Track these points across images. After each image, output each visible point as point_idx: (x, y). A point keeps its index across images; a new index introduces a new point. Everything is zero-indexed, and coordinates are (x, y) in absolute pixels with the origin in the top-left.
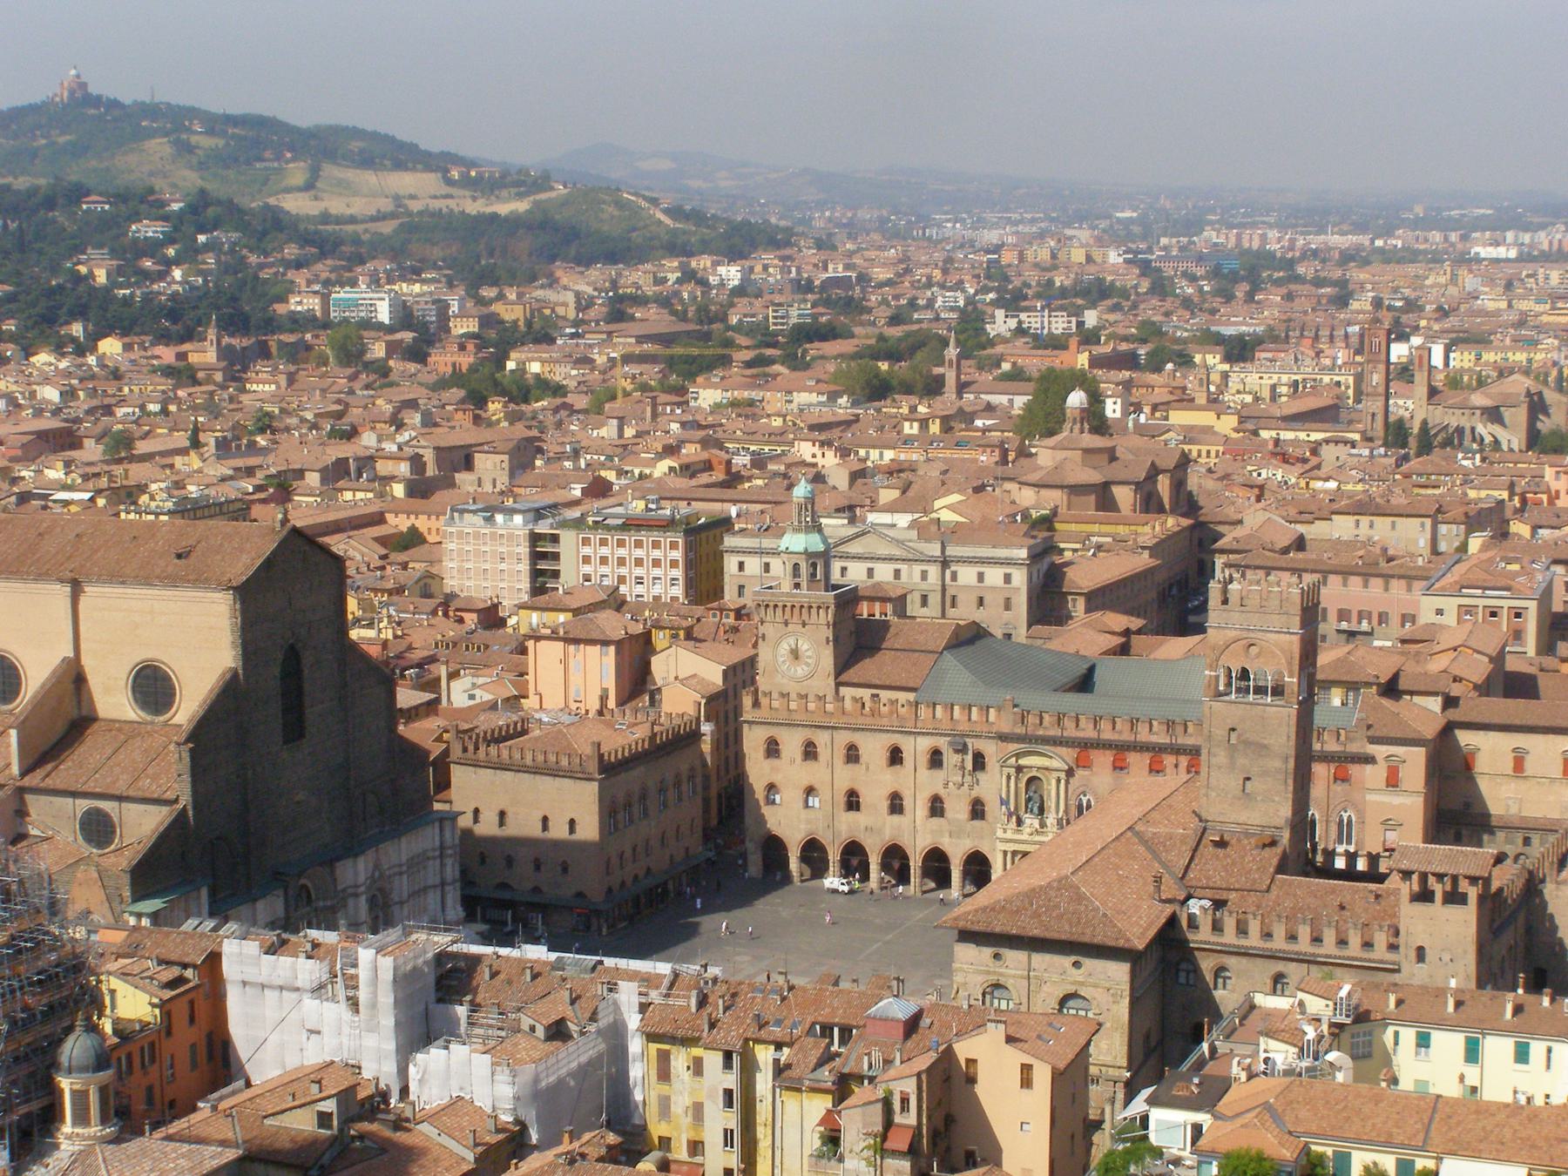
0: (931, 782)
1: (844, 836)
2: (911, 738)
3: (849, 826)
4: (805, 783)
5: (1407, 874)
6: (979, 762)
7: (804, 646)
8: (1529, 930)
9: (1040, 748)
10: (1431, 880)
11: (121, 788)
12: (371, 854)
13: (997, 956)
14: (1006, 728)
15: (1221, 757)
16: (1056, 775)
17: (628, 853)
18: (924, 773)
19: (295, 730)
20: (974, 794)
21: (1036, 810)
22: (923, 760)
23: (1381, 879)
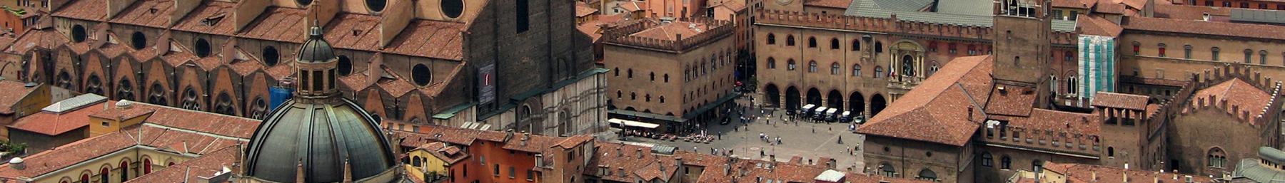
1: (808, 85)
3: (811, 79)
5: (1102, 108)
6: (879, 48)
8: (1168, 140)
10: (1115, 112)
11: (433, 54)
12: (561, 91)
13: (887, 149)
14: (891, 28)
15: (1003, 46)
17: (695, 93)
18: (850, 53)
19: (523, 25)
22: (849, 46)
23: (1090, 111)
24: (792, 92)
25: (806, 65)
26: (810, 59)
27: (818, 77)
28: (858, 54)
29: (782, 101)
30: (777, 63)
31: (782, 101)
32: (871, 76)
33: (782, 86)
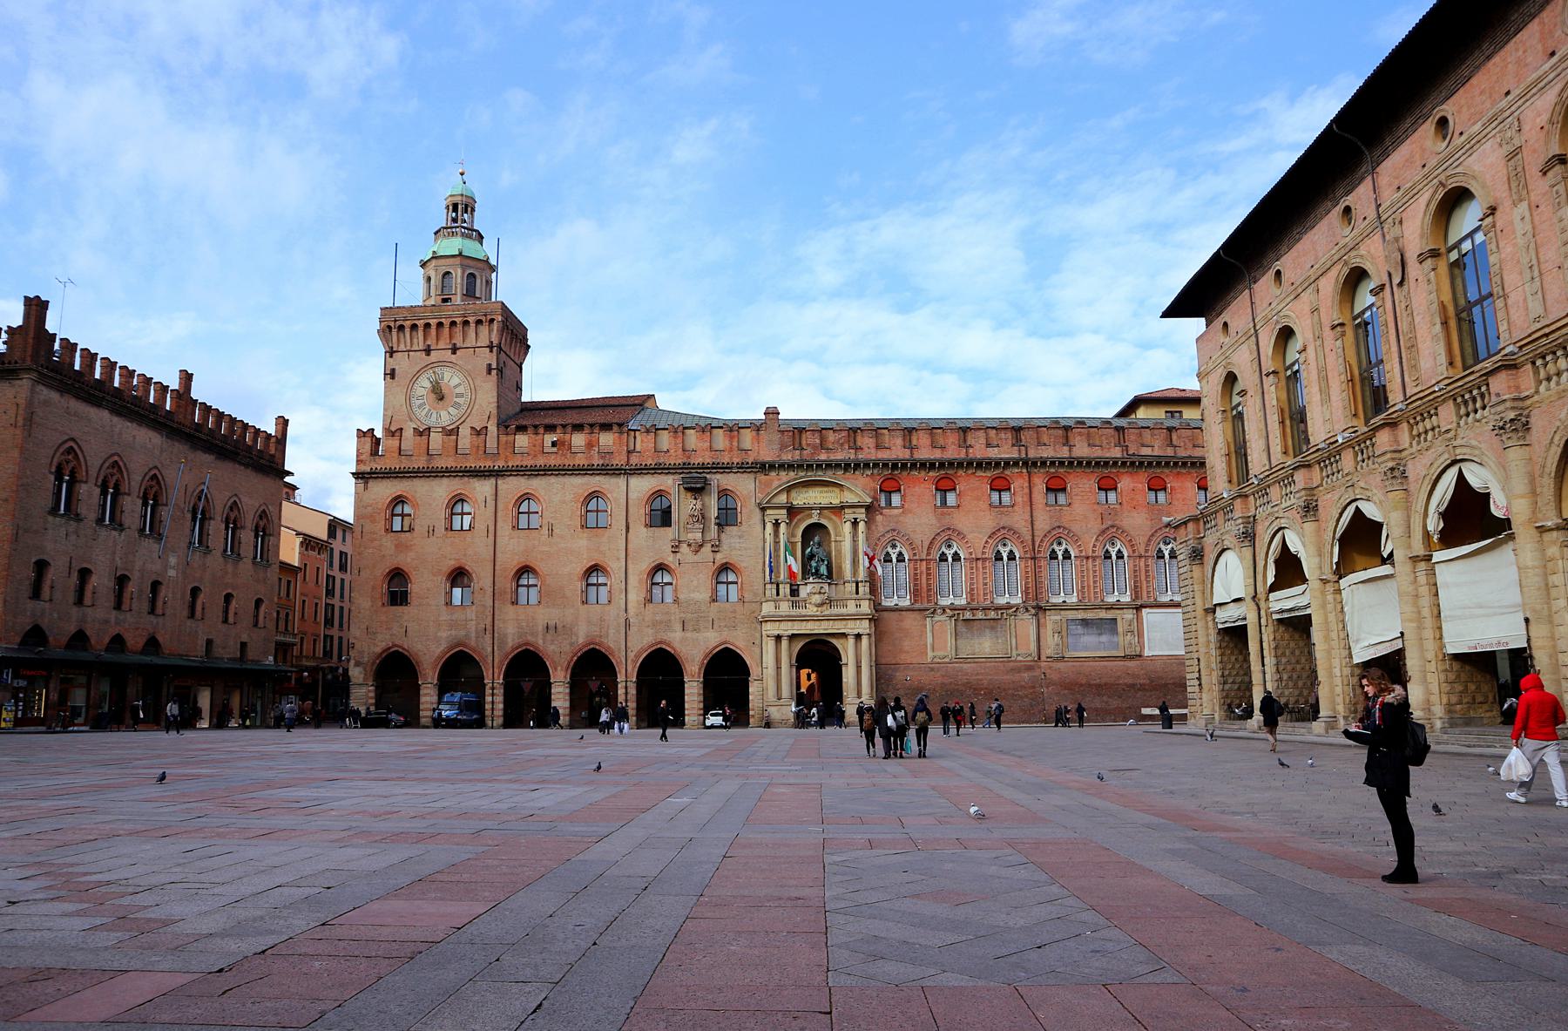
0: (651, 544)
2: (621, 481)
3: (521, 623)
4: (451, 564)
7: (451, 379)
9: (827, 476)
14: (767, 454)
16: (849, 515)
17: (101, 581)
18: (640, 533)
20: (720, 558)
21: (823, 570)
22: (639, 514)
24: (460, 669)
25: (506, 583)
27: (544, 615)
30: (415, 588)
32: (704, 595)
33: (429, 651)
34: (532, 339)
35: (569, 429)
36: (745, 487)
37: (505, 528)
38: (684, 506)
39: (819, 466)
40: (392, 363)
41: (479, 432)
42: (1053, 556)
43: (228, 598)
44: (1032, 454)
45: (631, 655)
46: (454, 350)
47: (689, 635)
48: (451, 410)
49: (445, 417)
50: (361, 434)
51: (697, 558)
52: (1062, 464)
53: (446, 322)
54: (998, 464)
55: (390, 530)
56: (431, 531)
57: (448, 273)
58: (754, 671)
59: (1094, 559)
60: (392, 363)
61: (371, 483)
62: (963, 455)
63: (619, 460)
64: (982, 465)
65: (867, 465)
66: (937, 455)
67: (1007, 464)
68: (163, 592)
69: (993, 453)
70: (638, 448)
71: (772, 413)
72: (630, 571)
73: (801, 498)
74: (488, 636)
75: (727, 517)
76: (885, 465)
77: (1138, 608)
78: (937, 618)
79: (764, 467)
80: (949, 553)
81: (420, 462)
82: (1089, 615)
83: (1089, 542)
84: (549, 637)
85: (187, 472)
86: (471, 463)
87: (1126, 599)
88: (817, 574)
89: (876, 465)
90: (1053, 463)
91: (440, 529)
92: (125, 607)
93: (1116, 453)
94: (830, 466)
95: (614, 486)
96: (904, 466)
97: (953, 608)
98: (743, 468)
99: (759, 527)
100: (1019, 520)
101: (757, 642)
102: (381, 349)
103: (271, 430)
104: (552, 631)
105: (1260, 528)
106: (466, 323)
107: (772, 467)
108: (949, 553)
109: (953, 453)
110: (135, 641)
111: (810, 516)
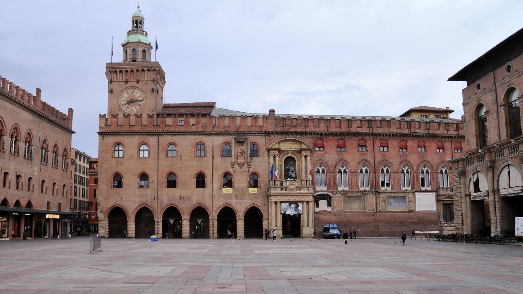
0: (223, 165)
2: (210, 138)
3: (168, 197)
4: (140, 171)
9: (294, 138)
14: (270, 127)
18: (218, 159)
21: (293, 175)
22: (217, 152)
24: (144, 215)
26: (168, 170)
28: (229, 160)
29: (131, 226)
30: (124, 181)
31: (131, 226)
34: (166, 76)
35: (189, 116)
36: (261, 141)
37: (162, 157)
38: (235, 149)
39: (292, 133)
40: (111, 86)
41: (151, 117)
42: (383, 171)
43: (54, 184)
44: (375, 131)
45: (215, 209)
46: (138, 81)
47: (238, 201)
48: (137, 107)
49: (134, 109)
50: (101, 116)
51: (242, 170)
52: (386, 135)
53: (135, 70)
54: (362, 134)
55: (113, 157)
56: (131, 157)
57: (134, 49)
58: (265, 216)
59: (398, 173)
60: (111, 86)
61: (105, 137)
62: (348, 131)
63: (209, 129)
64: (356, 134)
65: (310, 134)
66: (338, 130)
67: (365, 134)
68: (33, 182)
69: (360, 130)
70: (217, 124)
71: (272, 111)
72: (214, 175)
73: (284, 146)
74: (156, 200)
75: (254, 154)
76: (318, 134)
77: (414, 192)
78: (337, 195)
79: (267, 134)
80: (343, 169)
81: (126, 129)
82: (396, 195)
83: (396, 165)
84: (181, 201)
85: (42, 131)
86: (148, 129)
87: (409, 189)
88: (291, 177)
89: (314, 134)
90: (383, 135)
91: (135, 157)
92: (20, 188)
93: (406, 131)
94: (296, 133)
95: (208, 140)
96: (325, 134)
97: (344, 191)
98: (260, 133)
99: (267, 158)
100: (369, 157)
101: (266, 204)
102: (106, 81)
103: (66, 113)
104: (182, 199)
105: (497, 165)
106: (143, 70)
107: (272, 133)
108: (343, 169)
109: (344, 129)
110: (24, 203)
111: (288, 154)
